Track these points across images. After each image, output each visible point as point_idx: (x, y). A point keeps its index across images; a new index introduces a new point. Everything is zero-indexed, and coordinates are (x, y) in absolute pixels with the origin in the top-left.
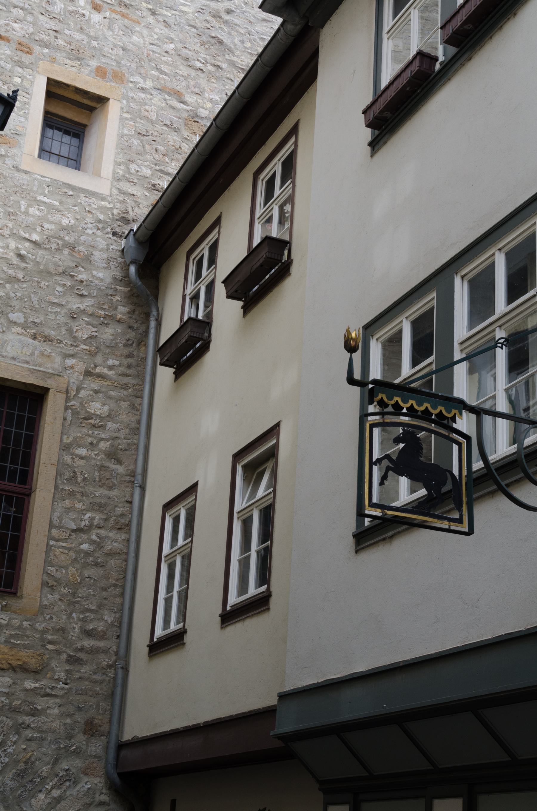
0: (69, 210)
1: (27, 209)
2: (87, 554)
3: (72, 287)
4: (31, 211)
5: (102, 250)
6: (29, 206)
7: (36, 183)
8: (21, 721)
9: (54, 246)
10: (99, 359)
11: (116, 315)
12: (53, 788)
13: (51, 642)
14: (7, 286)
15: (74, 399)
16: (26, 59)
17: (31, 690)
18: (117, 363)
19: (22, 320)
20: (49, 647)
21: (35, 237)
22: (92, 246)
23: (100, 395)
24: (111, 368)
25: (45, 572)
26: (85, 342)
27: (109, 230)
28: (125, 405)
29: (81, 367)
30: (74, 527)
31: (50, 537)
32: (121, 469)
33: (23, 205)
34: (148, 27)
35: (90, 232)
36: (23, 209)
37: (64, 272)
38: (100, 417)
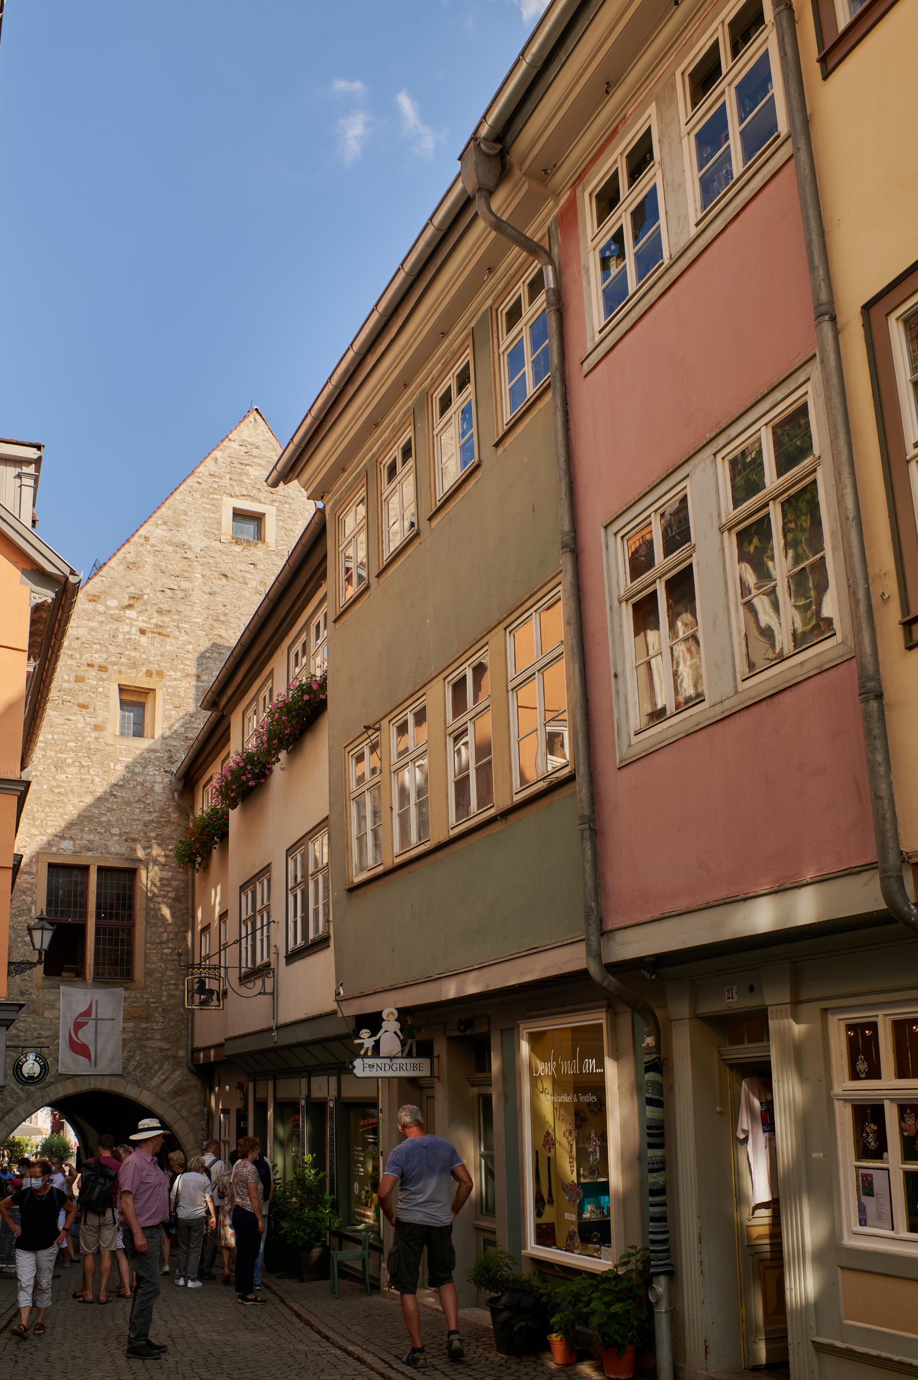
2: (167, 955)
3: (144, 808)
5: (159, 783)
6: (116, 765)
13: (153, 1003)
16: (104, 675)
17: (145, 1028)
19: (118, 832)
20: (152, 1005)
23: (167, 867)
25: (145, 967)
26: (154, 838)
27: (162, 770)
30: (159, 941)
31: (146, 949)
33: (112, 765)
35: (151, 773)
36: (112, 768)
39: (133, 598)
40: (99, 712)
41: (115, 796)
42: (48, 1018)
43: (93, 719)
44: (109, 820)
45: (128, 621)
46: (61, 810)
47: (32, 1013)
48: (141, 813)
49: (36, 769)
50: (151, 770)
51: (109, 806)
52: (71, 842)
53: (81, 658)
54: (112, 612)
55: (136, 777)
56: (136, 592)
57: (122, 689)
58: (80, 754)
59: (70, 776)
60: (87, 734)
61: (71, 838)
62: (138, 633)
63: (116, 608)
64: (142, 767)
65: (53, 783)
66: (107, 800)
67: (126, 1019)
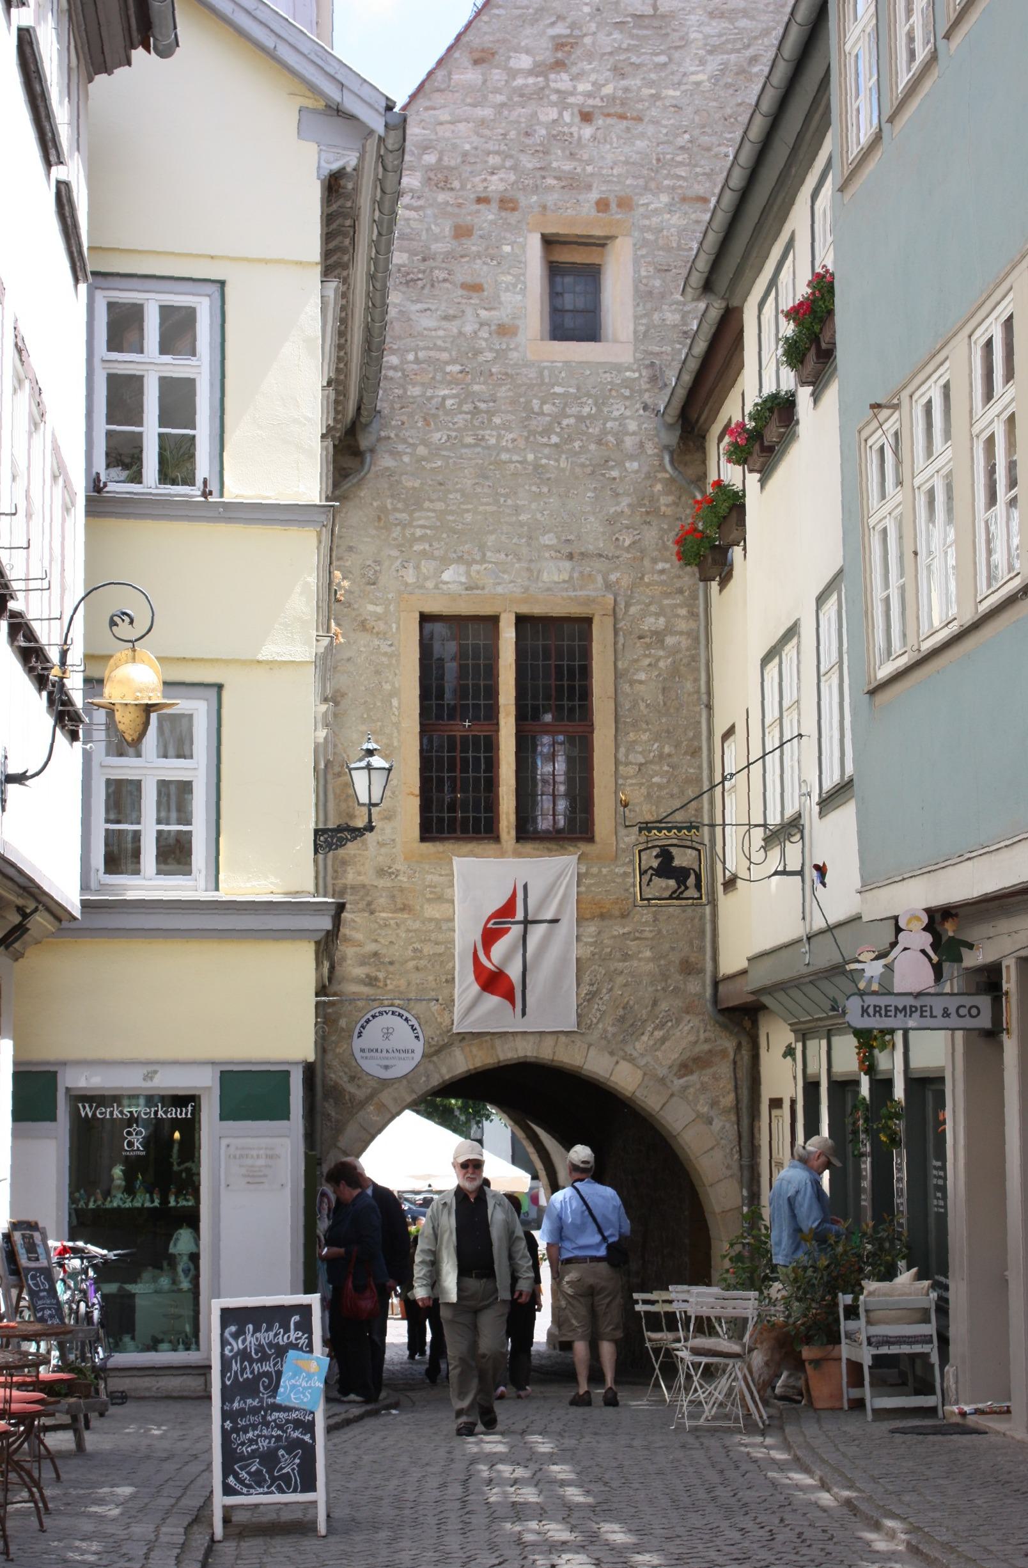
1: (541, 408)
2: (660, 787)
6: (543, 403)
8: (612, 969)
11: (659, 508)
12: (655, 1029)
14: (534, 506)
15: (623, 619)
16: (513, 218)
19: (554, 541)
21: (555, 439)
28: (683, 612)
33: (536, 404)
34: (655, 122)
35: (616, 414)
39: (563, 45)
40: (506, 297)
42: (431, 920)
43: (493, 313)
45: (554, 97)
50: (618, 409)
52: (462, 569)
53: (463, 187)
54: (519, 81)
56: (568, 31)
59: (454, 434)
60: (484, 344)
61: (460, 559)
62: (577, 119)
63: (530, 73)
64: (596, 404)
65: (422, 450)
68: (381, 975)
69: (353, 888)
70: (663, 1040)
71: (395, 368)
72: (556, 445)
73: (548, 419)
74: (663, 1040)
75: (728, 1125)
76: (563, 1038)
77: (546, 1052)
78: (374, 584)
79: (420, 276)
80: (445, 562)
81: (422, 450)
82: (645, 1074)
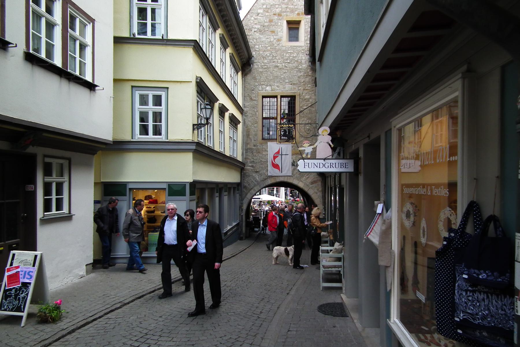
0: (295, 52)
4: (287, 55)
7: (287, 48)
9: (293, 62)
10: (306, 85)
12: (306, 176)
16: (280, 18)
18: (310, 86)
19: (288, 81)
21: (288, 61)
22: (302, 59)
23: (307, 94)
24: (309, 87)
26: (302, 83)
28: (313, 95)
29: (302, 89)
32: (314, 109)
33: (285, 54)
35: (301, 56)
37: (296, 68)
38: (308, 99)
40: (279, 33)
41: (286, 67)
42: (264, 155)
43: (277, 37)
44: (284, 77)
46: (266, 75)
47: (259, 152)
48: (296, 73)
49: (256, 60)
51: (284, 71)
53: (271, 12)
55: (294, 59)
57: (289, 23)
58: (273, 52)
59: (269, 61)
60: (275, 43)
61: (270, 85)
64: (297, 54)
65: (263, 64)
66: (283, 69)
67: (293, 155)
68: (254, 165)
69: (249, 149)
70: (308, 178)
71: (257, 48)
72: (289, 62)
73: (287, 57)
74: (308, 178)
75: (321, 194)
76: (289, 177)
77: (285, 180)
78: (253, 90)
79: (263, 30)
80: (267, 86)
81: (263, 64)
82: (305, 184)
